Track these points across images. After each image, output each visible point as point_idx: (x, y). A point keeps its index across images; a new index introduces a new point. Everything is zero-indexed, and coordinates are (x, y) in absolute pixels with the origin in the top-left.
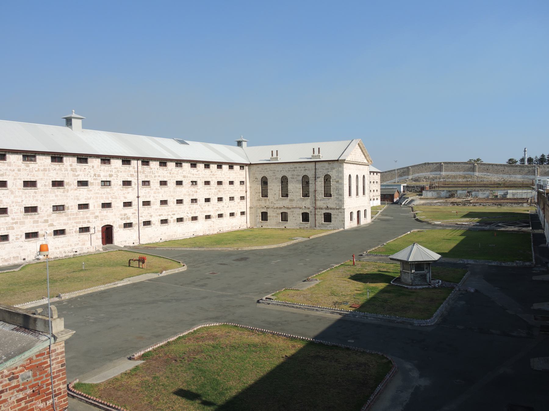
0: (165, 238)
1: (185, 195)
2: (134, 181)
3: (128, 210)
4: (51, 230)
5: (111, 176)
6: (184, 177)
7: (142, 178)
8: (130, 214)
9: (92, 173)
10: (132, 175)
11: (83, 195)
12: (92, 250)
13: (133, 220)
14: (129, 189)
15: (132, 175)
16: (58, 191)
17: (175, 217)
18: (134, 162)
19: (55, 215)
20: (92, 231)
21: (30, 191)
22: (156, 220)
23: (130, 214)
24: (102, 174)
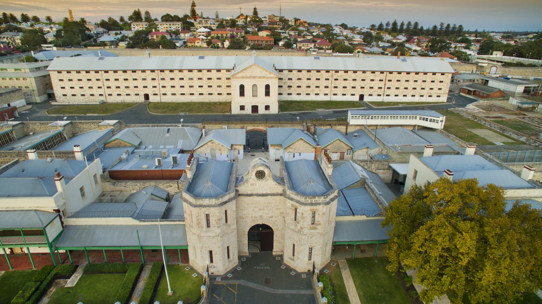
0: (174, 101)
1: (185, 84)
2: (157, 78)
3: (154, 89)
4: (125, 94)
5: (146, 77)
6: (184, 76)
7: (161, 77)
8: (156, 90)
9: (138, 76)
10: (155, 76)
11: (135, 83)
12: (140, 101)
13: (158, 93)
14: (155, 81)
15: (155, 76)
16: (126, 82)
17: (180, 93)
18: (156, 71)
19: (126, 89)
20: (140, 95)
21: (117, 82)
22: (169, 93)
23: (156, 91)
24: (142, 76)
